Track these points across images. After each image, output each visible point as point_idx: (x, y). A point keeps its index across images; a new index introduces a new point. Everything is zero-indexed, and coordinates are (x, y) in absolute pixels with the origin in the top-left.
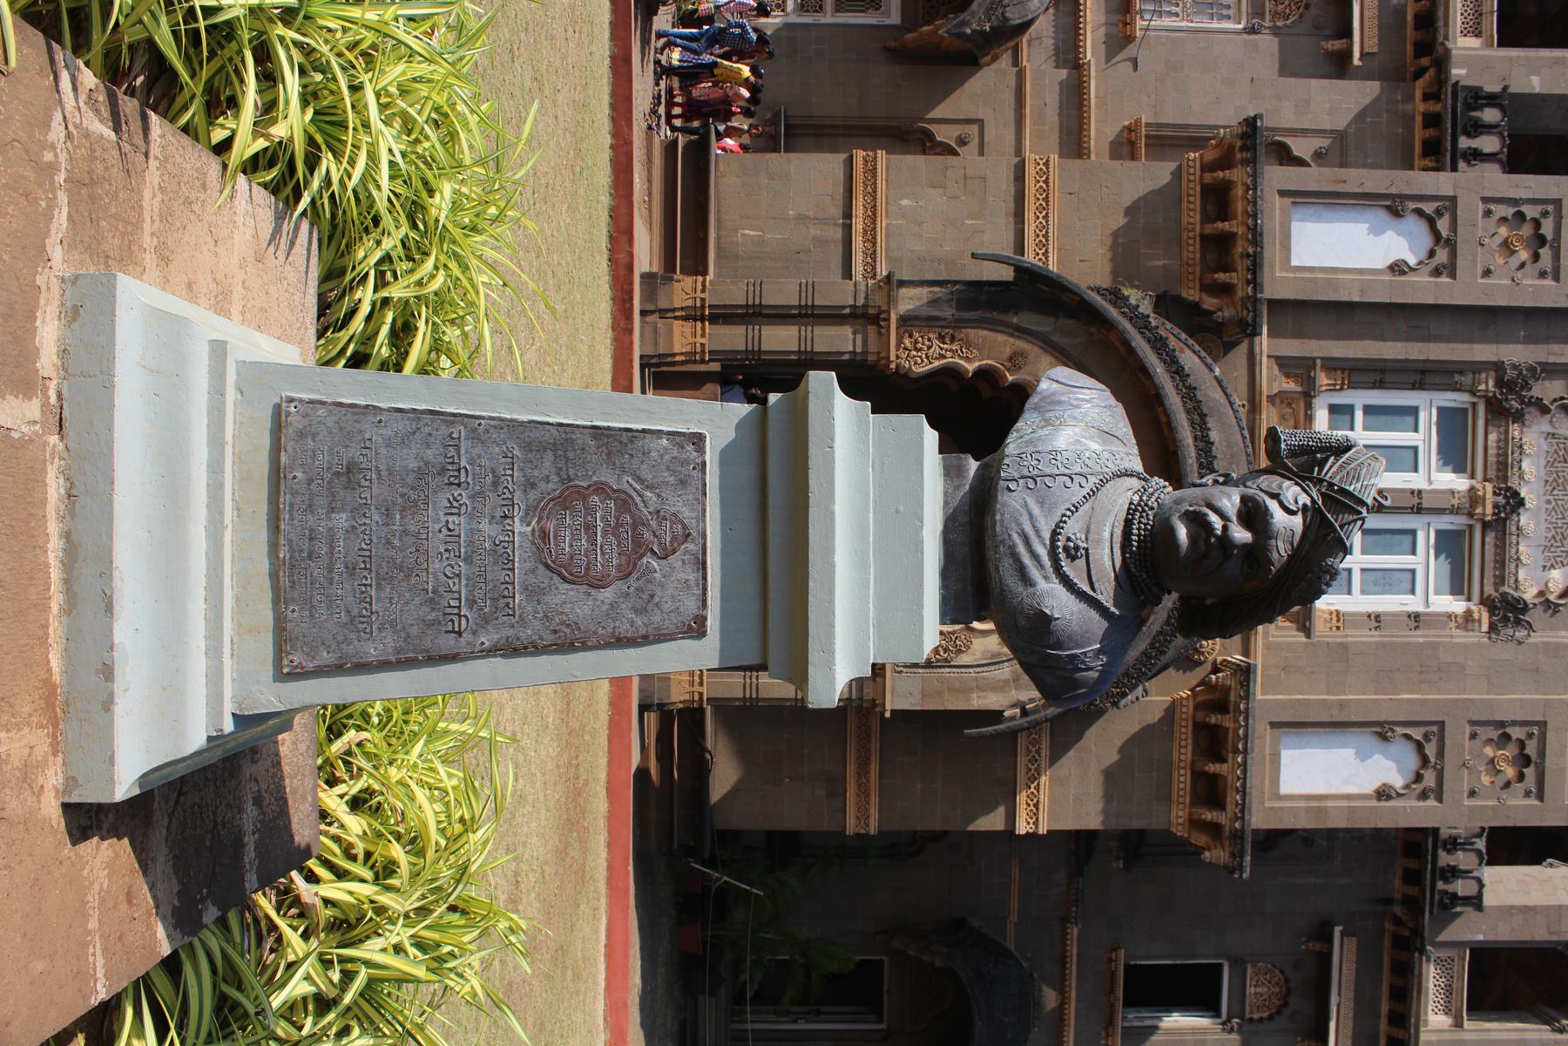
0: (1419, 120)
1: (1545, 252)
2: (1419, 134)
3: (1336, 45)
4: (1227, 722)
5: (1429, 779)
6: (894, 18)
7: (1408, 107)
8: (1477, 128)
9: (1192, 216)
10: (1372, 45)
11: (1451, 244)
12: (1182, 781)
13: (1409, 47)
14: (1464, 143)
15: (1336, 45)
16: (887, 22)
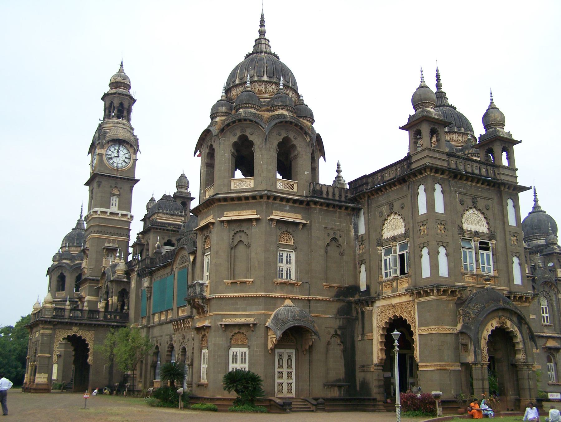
0: (321, 207)
1: (443, 223)
2: (324, 208)
3: (301, 227)
4: (518, 296)
5: (518, 255)
6: (294, 351)
7: (317, 209)
8: (321, 192)
9: (444, 297)
10: (300, 216)
11: (443, 243)
12: (523, 304)
13: (300, 206)
14: (324, 196)
15: (301, 227)
16: (294, 353)
